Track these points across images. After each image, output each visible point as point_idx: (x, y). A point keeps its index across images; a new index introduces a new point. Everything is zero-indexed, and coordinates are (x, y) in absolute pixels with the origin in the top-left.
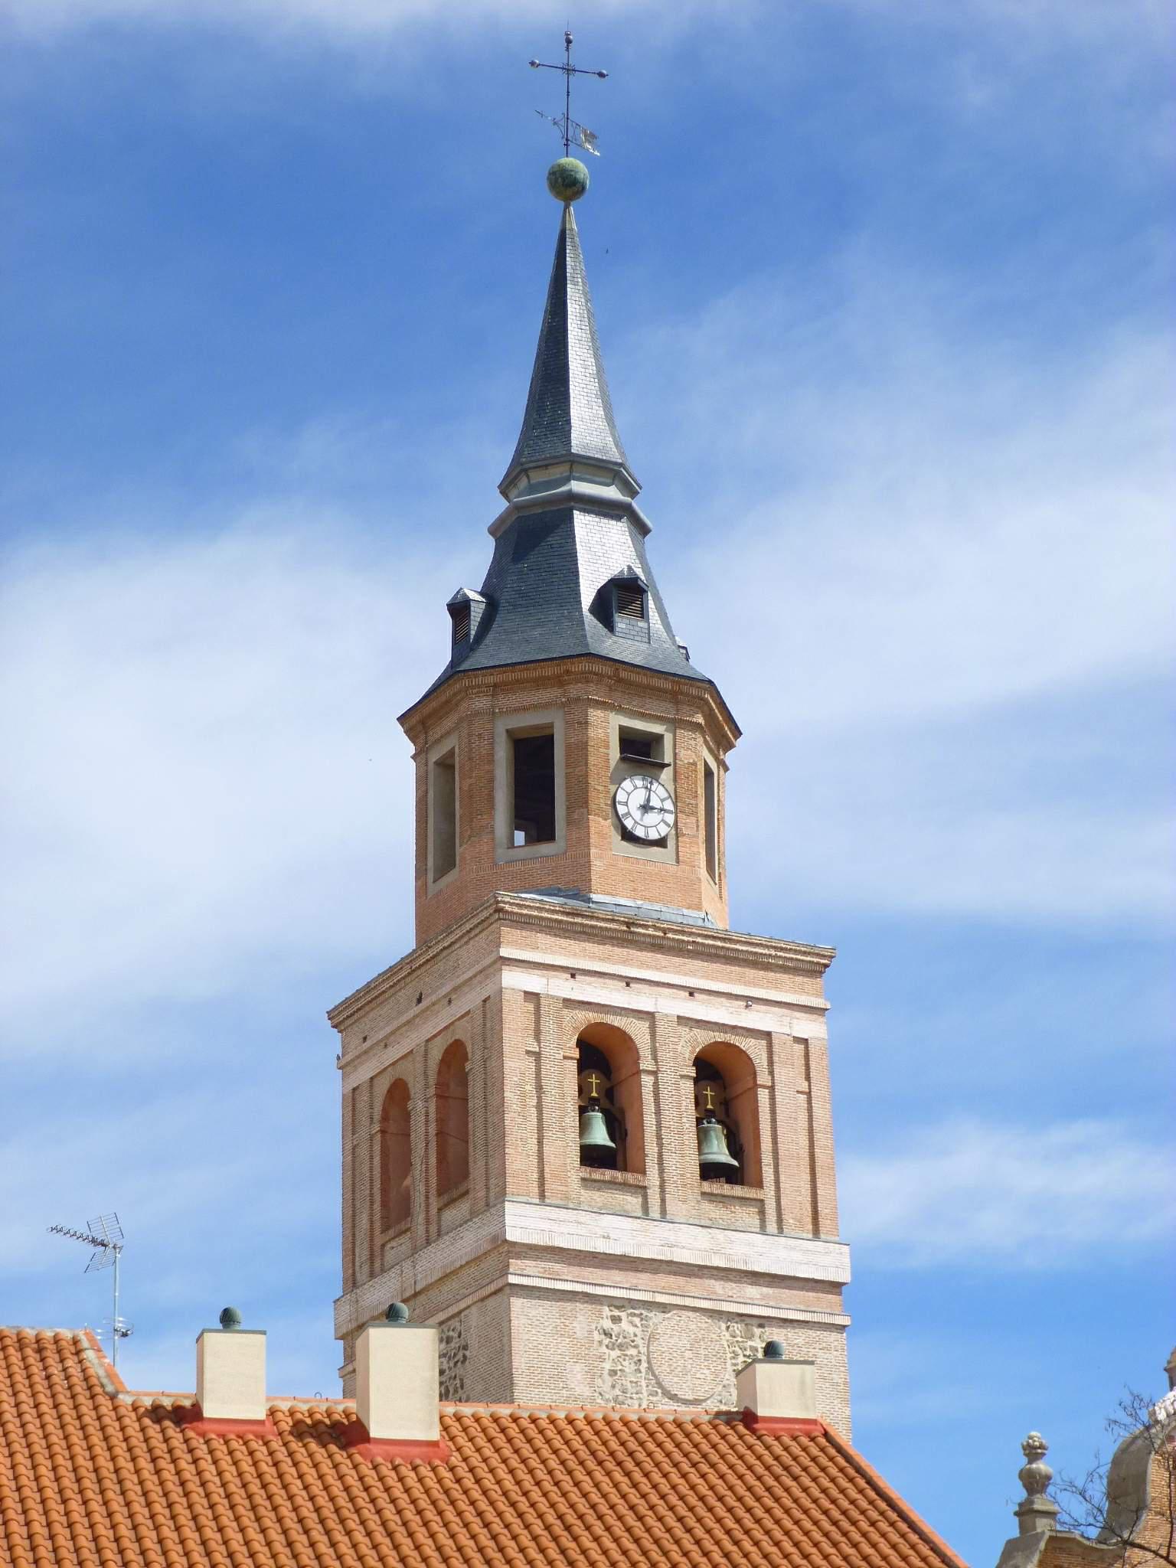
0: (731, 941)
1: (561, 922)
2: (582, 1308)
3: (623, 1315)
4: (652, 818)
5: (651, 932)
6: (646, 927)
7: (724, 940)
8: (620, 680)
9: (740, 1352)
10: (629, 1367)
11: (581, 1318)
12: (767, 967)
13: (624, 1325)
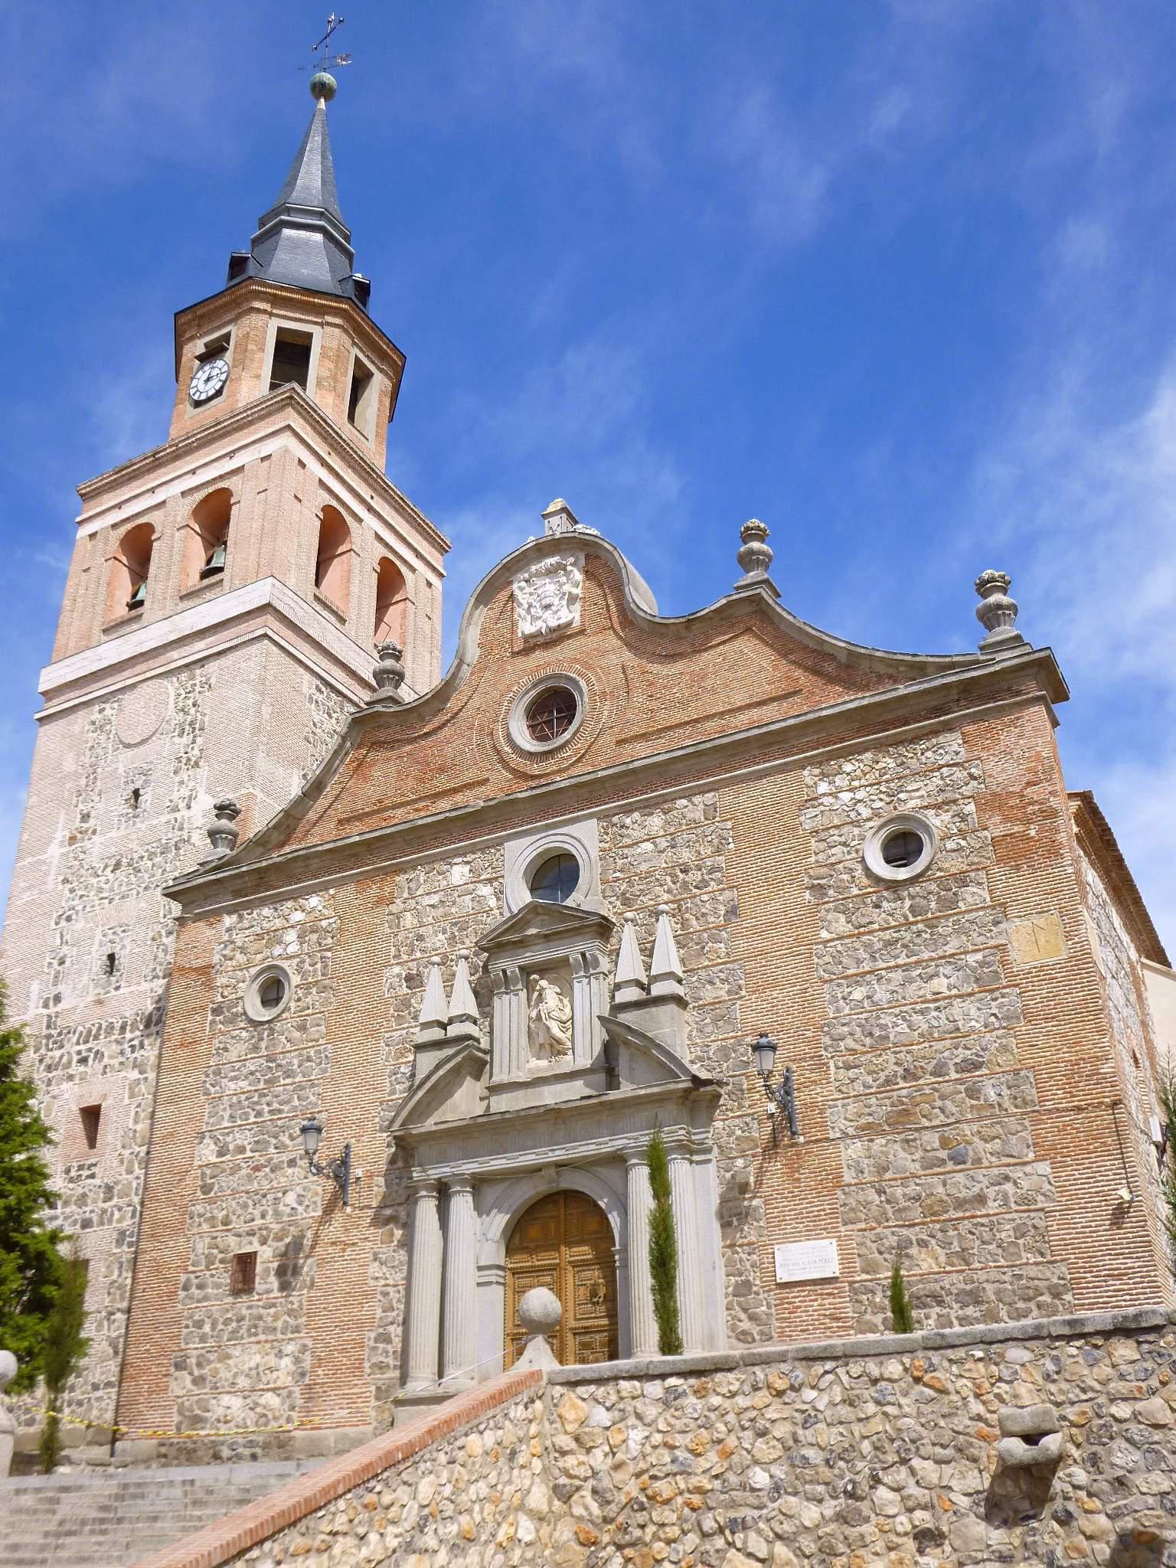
0: (219, 423)
1: (115, 480)
2: (81, 714)
3: (107, 706)
4: (211, 384)
5: (168, 451)
6: (165, 449)
7: (216, 425)
8: (202, 317)
9: (182, 692)
10: (103, 737)
11: (79, 720)
12: (251, 423)
13: (108, 712)
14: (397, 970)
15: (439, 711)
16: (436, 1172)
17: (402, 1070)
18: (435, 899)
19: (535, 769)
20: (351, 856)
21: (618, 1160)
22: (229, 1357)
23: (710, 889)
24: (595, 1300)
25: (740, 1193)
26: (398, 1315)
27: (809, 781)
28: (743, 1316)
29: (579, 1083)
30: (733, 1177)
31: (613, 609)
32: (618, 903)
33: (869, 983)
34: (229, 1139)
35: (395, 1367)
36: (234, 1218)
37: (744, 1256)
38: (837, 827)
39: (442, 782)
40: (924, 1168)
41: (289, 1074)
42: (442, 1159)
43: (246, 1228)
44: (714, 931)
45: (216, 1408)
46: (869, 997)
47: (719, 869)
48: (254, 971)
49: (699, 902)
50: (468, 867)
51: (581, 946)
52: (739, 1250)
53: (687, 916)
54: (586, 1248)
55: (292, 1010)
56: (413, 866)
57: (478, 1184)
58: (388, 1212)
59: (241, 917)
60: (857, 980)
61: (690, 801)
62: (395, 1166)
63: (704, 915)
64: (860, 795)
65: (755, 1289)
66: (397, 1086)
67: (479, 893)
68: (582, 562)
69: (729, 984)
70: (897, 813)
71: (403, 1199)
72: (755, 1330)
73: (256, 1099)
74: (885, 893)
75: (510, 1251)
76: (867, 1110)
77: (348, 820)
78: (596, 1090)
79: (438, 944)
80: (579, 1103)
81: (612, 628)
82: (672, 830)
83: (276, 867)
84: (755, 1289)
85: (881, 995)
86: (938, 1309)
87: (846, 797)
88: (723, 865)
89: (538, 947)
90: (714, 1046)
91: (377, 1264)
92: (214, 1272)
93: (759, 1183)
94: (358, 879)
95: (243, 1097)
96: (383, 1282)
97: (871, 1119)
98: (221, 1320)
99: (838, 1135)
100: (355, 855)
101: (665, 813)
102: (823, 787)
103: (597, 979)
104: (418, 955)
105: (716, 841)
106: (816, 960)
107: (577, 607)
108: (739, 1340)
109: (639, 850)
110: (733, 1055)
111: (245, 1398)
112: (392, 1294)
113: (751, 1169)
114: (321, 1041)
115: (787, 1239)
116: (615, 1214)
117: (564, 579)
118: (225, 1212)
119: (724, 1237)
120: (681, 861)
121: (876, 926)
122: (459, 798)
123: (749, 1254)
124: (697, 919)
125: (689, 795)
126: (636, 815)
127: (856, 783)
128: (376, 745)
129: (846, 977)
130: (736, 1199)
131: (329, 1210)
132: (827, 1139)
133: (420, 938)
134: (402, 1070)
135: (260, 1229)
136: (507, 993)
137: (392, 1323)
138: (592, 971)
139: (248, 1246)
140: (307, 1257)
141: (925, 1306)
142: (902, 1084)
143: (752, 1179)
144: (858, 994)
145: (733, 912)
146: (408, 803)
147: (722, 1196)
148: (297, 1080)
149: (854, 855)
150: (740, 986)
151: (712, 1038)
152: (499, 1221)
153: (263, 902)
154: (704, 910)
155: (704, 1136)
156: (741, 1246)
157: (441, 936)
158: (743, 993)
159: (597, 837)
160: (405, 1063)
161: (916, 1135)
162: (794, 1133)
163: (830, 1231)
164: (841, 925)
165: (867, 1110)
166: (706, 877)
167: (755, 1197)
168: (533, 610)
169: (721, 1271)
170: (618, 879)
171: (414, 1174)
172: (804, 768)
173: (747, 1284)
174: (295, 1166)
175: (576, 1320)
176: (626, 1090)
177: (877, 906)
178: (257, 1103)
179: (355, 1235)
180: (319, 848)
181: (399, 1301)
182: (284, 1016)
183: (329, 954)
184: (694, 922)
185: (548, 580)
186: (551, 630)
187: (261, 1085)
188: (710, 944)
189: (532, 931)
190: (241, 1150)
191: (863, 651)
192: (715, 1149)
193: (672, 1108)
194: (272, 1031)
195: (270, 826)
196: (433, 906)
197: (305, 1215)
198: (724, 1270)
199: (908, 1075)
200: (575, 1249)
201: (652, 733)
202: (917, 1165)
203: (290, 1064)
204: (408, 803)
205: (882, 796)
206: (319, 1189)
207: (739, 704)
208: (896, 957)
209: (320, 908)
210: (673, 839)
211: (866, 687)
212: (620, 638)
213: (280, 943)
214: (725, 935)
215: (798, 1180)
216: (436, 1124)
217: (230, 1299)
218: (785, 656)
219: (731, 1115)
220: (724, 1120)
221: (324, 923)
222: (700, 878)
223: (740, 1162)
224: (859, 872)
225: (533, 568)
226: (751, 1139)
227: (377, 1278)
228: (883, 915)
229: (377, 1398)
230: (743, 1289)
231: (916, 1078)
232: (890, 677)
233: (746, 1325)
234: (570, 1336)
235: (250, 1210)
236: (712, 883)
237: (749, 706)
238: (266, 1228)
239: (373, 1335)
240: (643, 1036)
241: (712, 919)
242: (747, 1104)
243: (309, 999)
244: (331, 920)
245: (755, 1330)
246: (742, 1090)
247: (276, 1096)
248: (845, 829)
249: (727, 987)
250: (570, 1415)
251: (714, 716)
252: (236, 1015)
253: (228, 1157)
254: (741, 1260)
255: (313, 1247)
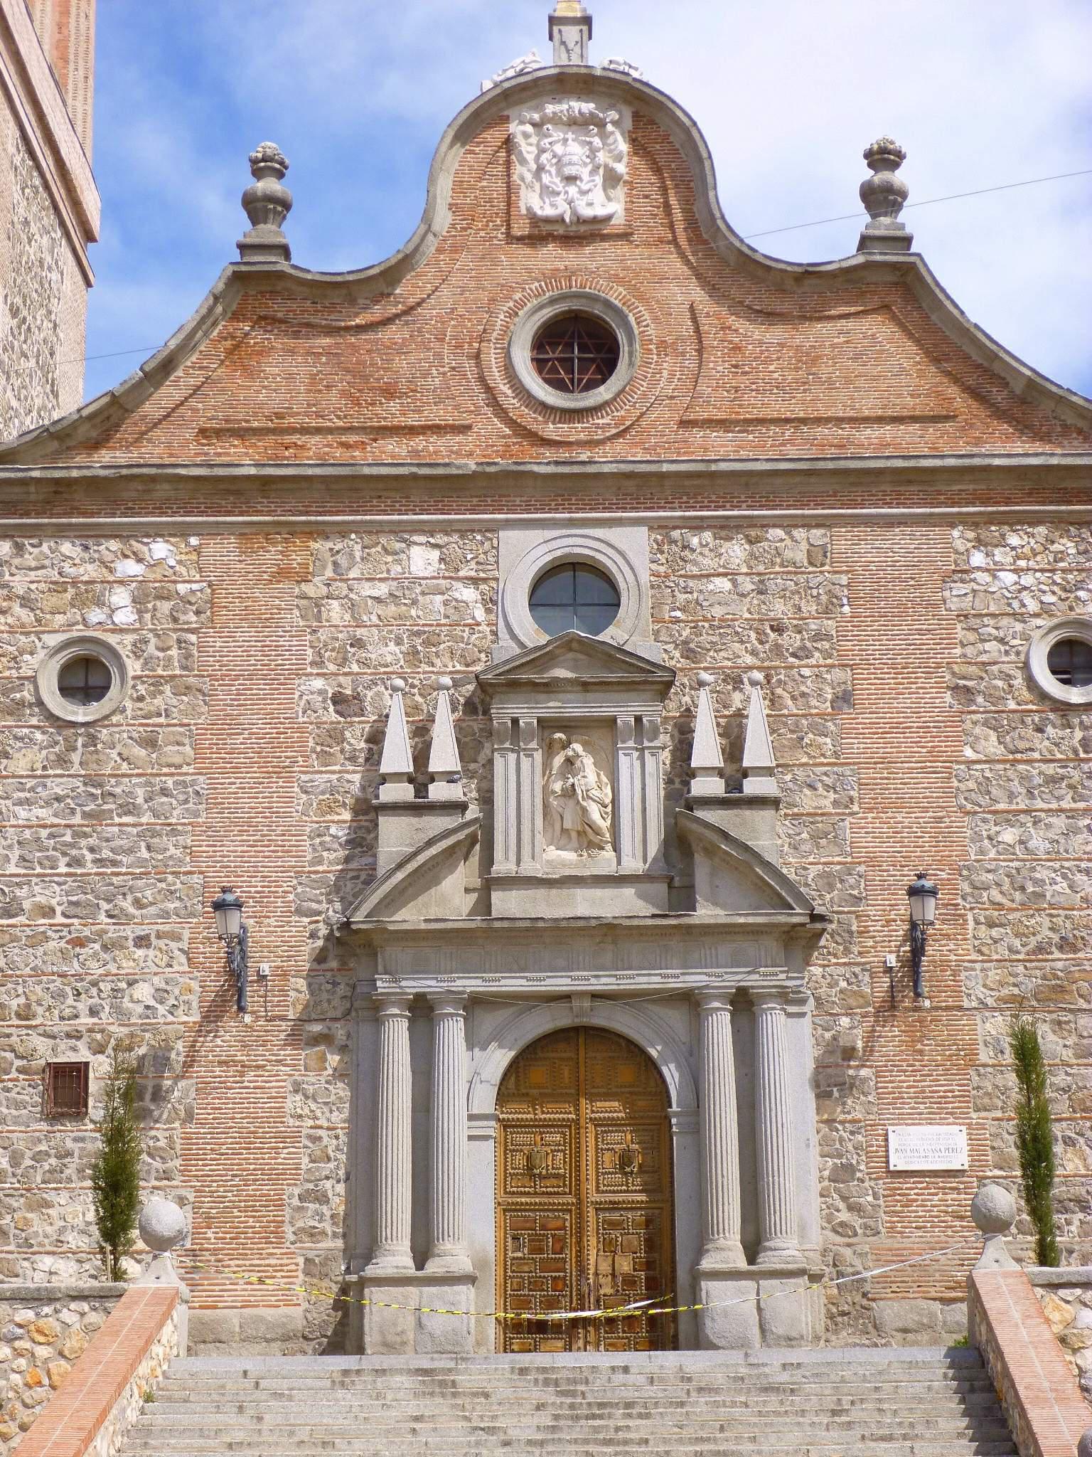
14: (318, 683)
15: (382, 295)
16: (413, 985)
17: (333, 830)
18: (382, 590)
19: (551, 430)
20: (229, 492)
21: (691, 1001)
22: (49, 1205)
23: (812, 661)
24: (628, 1169)
25: (843, 1059)
26: (337, 1168)
27: (960, 545)
28: (842, 1205)
29: (629, 892)
30: (834, 1038)
31: (678, 214)
32: (677, 654)
33: (1022, 825)
34: (22, 893)
35: (335, 1235)
36: (40, 1010)
37: (845, 1135)
38: (993, 615)
39: (392, 412)
40: (1078, 1056)
41: (129, 808)
42: (420, 968)
43: (65, 1027)
44: (817, 719)
45: (29, 1273)
46: (1021, 842)
47: (828, 637)
48: (53, 640)
49: (797, 677)
50: (435, 554)
51: (637, 708)
52: (840, 1127)
53: (779, 691)
54: (616, 1104)
55: (129, 712)
56: (343, 531)
57: (474, 1004)
58: (317, 1028)
59: (19, 549)
60: (1008, 818)
61: (789, 533)
62: (323, 966)
63: (803, 695)
64: (1027, 580)
65: (859, 1175)
66: (325, 854)
67: (457, 595)
68: (628, 123)
69: (836, 792)
70: (1073, 615)
71: (338, 1014)
72: (857, 1222)
73: (68, 838)
74: (1052, 716)
75: (504, 1095)
76: (1012, 980)
77: (218, 433)
78: (658, 907)
79: (389, 659)
80: (650, 922)
81: (674, 241)
82: (761, 568)
83: (93, 484)
84: (859, 1175)
85: (1038, 842)
86: (1081, 1216)
87: (1008, 578)
88: (833, 633)
89: (569, 696)
90: (813, 871)
91: (298, 1097)
92: (10, 1085)
93: (869, 1050)
94: (245, 534)
95: (44, 833)
96: (311, 1123)
97: (1016, 991)
98: (29, 1154)
99: (974, 1004)
100: (237, 493)
101: (750, 542)
102: (978, 559)
103: (653, 755)
104: (355, 668)
105: (824, 598)
106: (956, 784)
107: (620, 192)
108: (837, 1233)
109: (711, 587)
110: (839, 885)
111: (79, 1261)
112: (326, 1140)
113: (859, 1032)
114: (185, 769)
115: (901, 1120)
116: (672, 1066)
117: (597, 141)
118: (22, 1000)
119: (818, 1109)
120: (772, 614)
121: (1036, 755)
122: (419, 442)
123: (852, 1133)
124: (793, 698)
125: (789, 524)
126: (707, 536)
127: (1022, 563)
128: (267, 321)
129: (995, 812)
130: (837, 1065)
131: (212, 1015)
132: (960, 1008)
133: (358, 643)
134: (333, 830)
135: (90, 1031)
136: (513, 751)
137: (327, 1178)
138: (646, 744)
139: (70, 1053)
140: (177, 1078)
141: (1067, 1211)
142: (1057, 955)
143: (860, 1044)
144: (1009, 836)
145: (844, 699)
146: (330, 431)
147: (816, 1060)
148: (144, 820)
149: (1013, 657)
150: (851, 799)
151: (811, 859)
152: (498, 1059)
153: (61, 532)
154: (803, 688)
155: (798, 982)
156: (842, 1122)
157: (392, 646)
158: (856, 808)
159: (648, 556)
160: (338, 822)
161: (1071, 1017)
162: (918, 995)
163: (955, 1116)
164: (992, 745)
165: (1012, 980)
166: (808, 644)
167: (863, 1066)
168: (546, 178)
169: (815, 1151)
170: (677, 621)
171: (379, 984)
172: (953, 526)
173: (850, 1169)
174: (148, 946)
175: (598, 1191)
176: (705, 913)
177: (1040, 730)
178: (72, 846)
179: (260, 1055)
180: (183, 471)
181: (338, 1149)
182: (114, 719)
183: (193, 638)
184: (790, 702)
185: (570, 136)
186: (580, 221)
187: (77, 820)
188: (811, 735)
189: (561, 673)
190: (49, 912)
191: (1054, 389)
192: (811, 1001)
193: (771, 945)
194: (93, 740)
195: (85, 413)
196: (378, 600)
197: (170, 1018)
198: (818, 1148)
199: (1066, 945)
200: (599, 1104)
201: (737, 422)
202: (1070, 1052)
203: (130, 794)
204: (330, 431)
205: (1055, 588)
206: (195, 985)
207: (866, 413)
208: (1059, 799)
209: (172, 563)
210: (761, 582)
211: (1044, 437)
212: (687, 262)
213: (100, 603)
214: (833, 728)
215: (921, 1052)
216: (426, 921)
217: (44, 1126)
218: (936, 361)
219: (834, 961)
220: (824, 966)
221: (182, 588)
222: (798, 643)
223: (845, 1021)
224: (1018, 682)
225: (550, 109)
226: (861, 995)
227: (300, 1116)
228: (1046, 743)
229: (307, 1274)
230: (843, 1173)
231: (1075, 949)
232: (1080, 432)
233: (844, 1216)
234: (591, 1210)
235: (70, 1001)
236: (817, 654)
237: (880, 420)
238: (102, 1031)
239: (297, 1191)
240: (747, 848)
241: (814, 702)
242: (856, 949)
243: (158, 701)
244: (195, 586)
245: (857, 1222)
246: (851, 933)
247: (108, 840)
248: (1005, 622)
249: (832, 796)
250: (1055, 1316)
251: (828, 420)
252: (21, 704)
253: (21, 919)
254: (841, 1140)
255: (188, 1065)
